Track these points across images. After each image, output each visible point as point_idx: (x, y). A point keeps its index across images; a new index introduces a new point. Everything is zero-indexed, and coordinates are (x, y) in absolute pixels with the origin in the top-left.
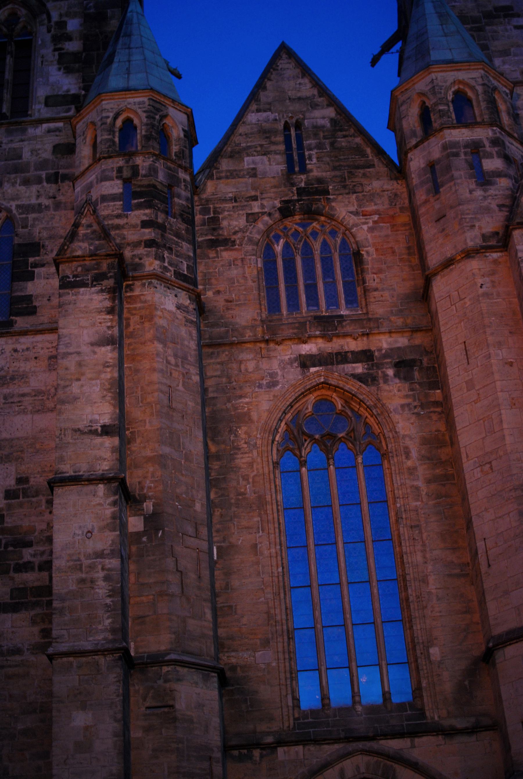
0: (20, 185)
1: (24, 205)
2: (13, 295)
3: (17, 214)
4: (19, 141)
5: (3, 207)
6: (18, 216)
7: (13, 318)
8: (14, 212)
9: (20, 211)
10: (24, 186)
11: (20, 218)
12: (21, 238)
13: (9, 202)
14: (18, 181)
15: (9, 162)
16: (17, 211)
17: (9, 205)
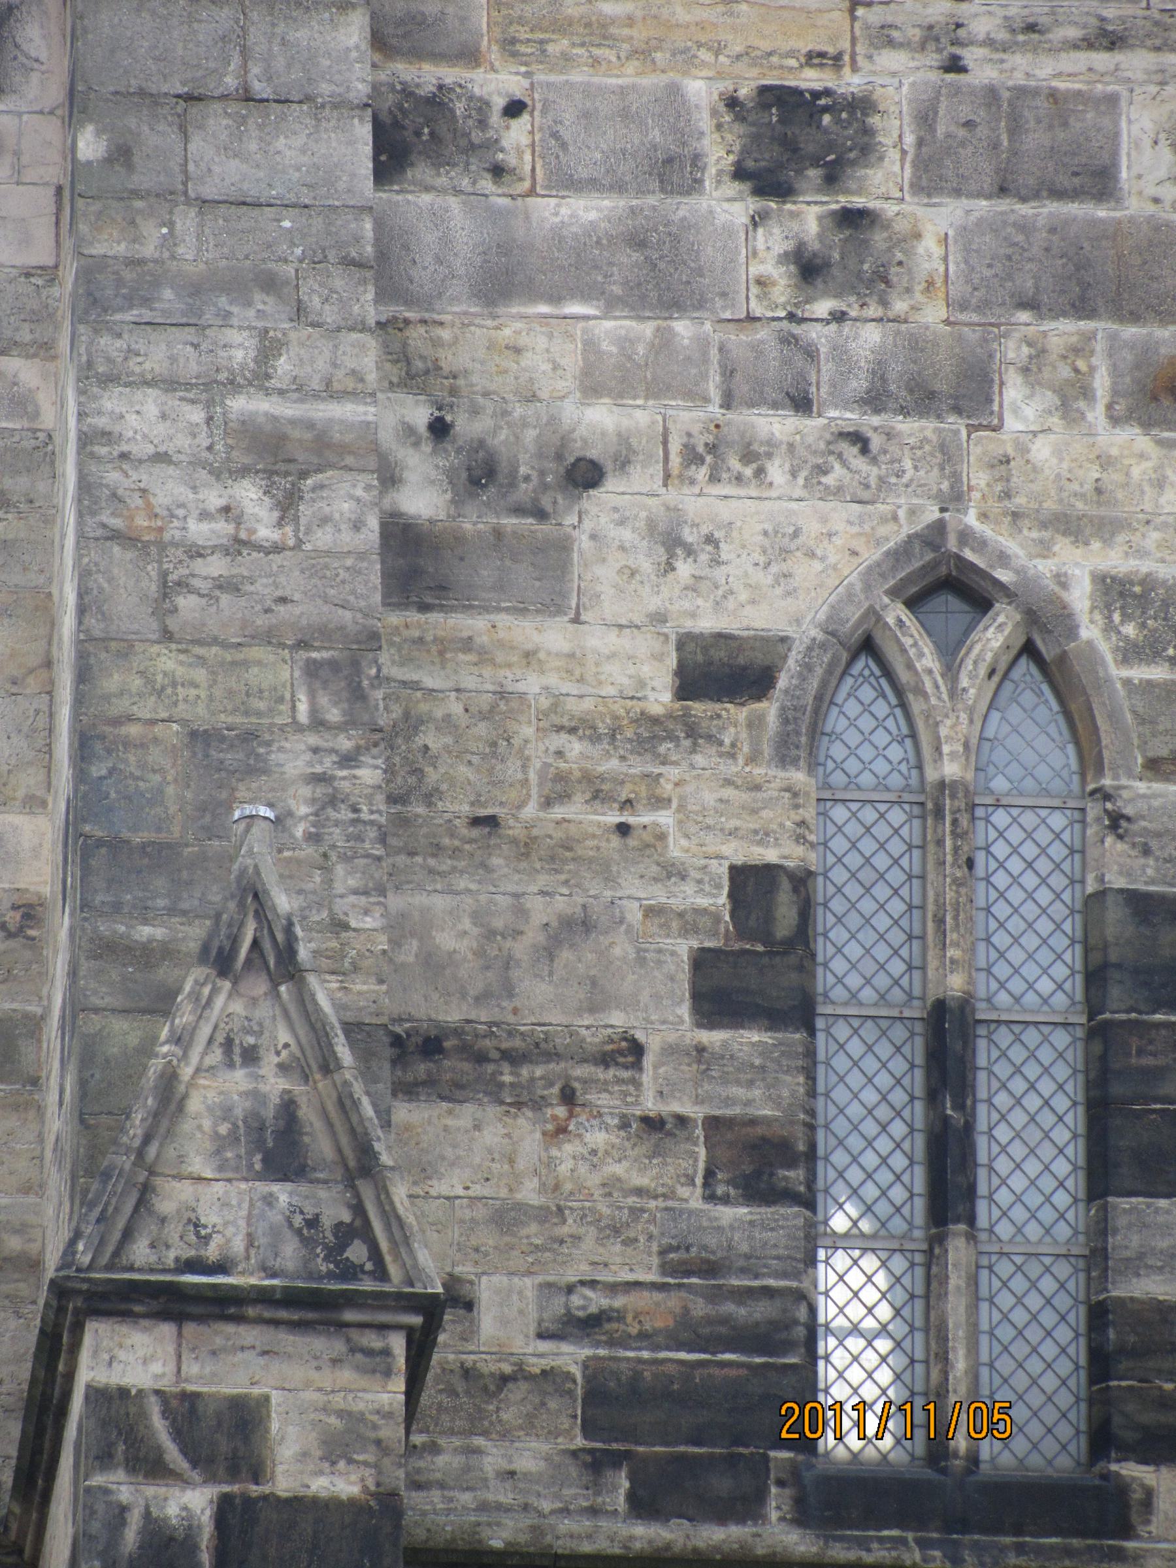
0: (1115, 420)
1: (1149, 582)
2: (1119, 1291)
3: (1104, 648)
4: (1089, 44)
5: (1004, 576)
6: (1118, 672)
7: (1132, 1470)
8: (1090, 631)
9: (1130, 630)
10: (1147, 425)
11: (1127, 682)
12: (1146, 851)
13: (1044, 549)
14: (1101, 383)
15: (1025, 210)
16: (1109, 628)
17: (1044, 567)
